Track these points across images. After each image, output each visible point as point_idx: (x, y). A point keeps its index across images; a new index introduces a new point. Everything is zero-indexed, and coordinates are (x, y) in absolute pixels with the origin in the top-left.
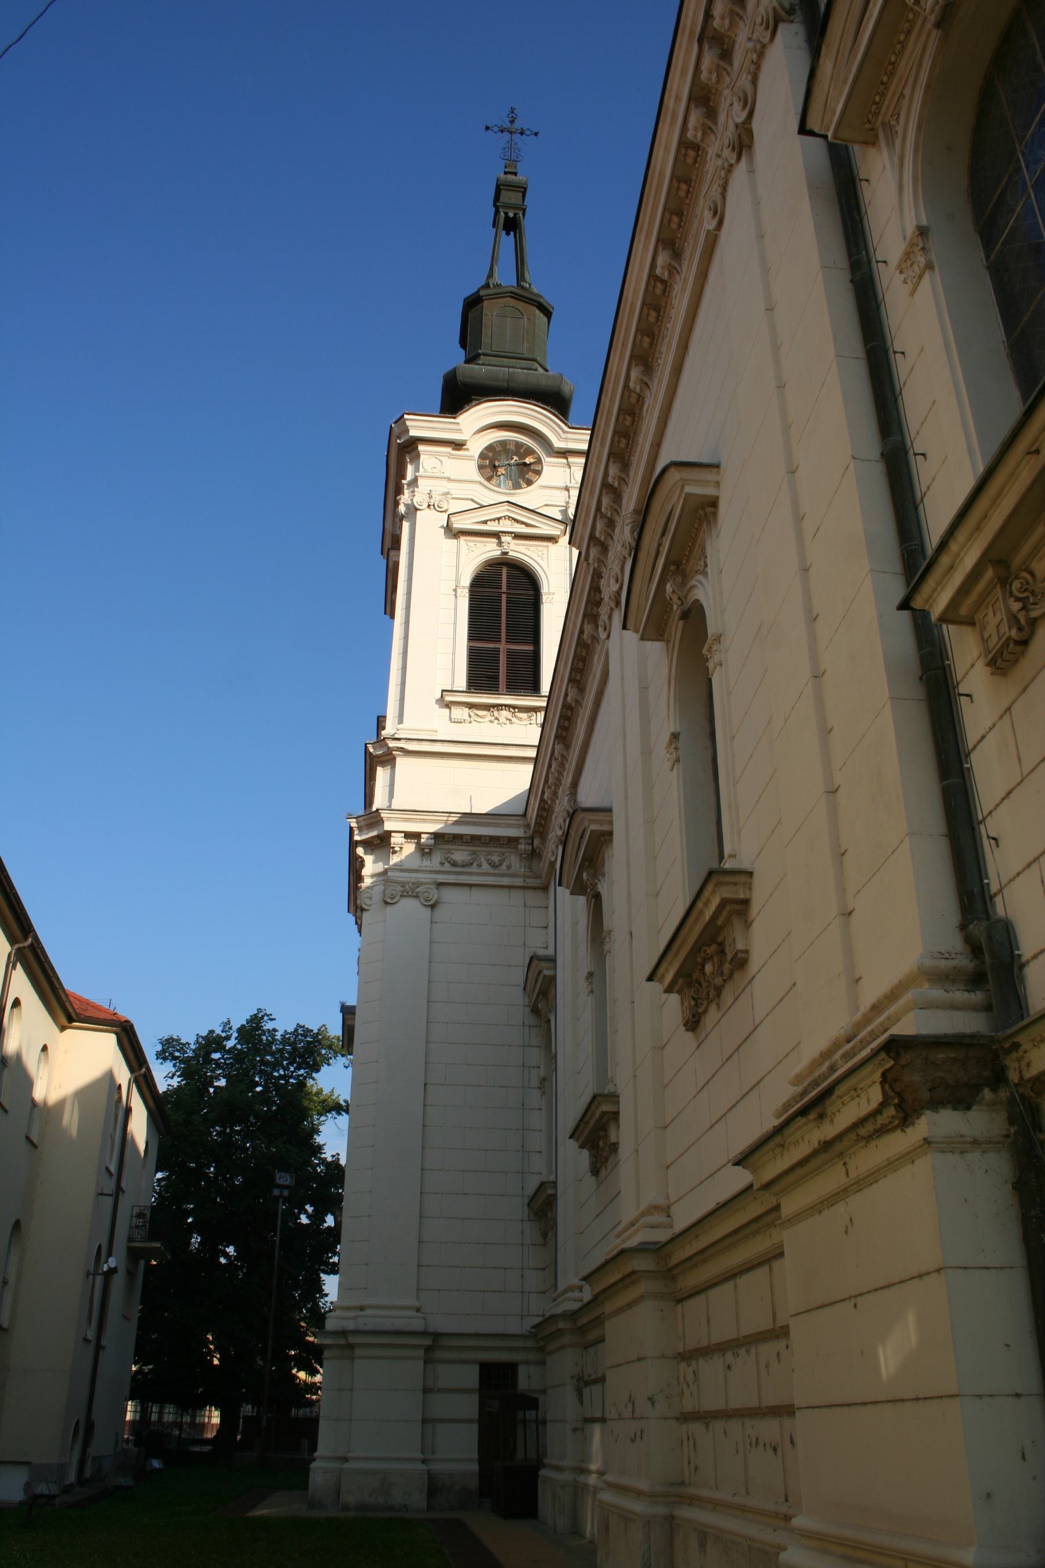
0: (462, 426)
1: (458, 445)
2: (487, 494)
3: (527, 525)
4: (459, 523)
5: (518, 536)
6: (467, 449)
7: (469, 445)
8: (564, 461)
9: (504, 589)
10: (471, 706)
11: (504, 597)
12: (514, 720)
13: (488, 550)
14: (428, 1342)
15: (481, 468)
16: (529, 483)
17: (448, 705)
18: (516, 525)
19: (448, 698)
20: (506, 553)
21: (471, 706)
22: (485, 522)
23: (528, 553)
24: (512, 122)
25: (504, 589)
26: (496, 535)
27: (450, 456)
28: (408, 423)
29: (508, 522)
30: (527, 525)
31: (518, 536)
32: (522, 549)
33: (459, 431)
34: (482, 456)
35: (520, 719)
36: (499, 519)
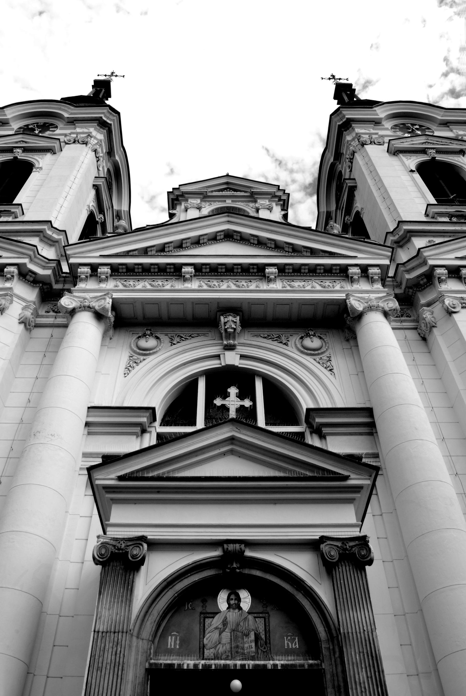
20: (16, 158)
23: (31, 156)
26: (10, 150)
31: (26, 150)
33: (5, 115)
34: (20, 128)
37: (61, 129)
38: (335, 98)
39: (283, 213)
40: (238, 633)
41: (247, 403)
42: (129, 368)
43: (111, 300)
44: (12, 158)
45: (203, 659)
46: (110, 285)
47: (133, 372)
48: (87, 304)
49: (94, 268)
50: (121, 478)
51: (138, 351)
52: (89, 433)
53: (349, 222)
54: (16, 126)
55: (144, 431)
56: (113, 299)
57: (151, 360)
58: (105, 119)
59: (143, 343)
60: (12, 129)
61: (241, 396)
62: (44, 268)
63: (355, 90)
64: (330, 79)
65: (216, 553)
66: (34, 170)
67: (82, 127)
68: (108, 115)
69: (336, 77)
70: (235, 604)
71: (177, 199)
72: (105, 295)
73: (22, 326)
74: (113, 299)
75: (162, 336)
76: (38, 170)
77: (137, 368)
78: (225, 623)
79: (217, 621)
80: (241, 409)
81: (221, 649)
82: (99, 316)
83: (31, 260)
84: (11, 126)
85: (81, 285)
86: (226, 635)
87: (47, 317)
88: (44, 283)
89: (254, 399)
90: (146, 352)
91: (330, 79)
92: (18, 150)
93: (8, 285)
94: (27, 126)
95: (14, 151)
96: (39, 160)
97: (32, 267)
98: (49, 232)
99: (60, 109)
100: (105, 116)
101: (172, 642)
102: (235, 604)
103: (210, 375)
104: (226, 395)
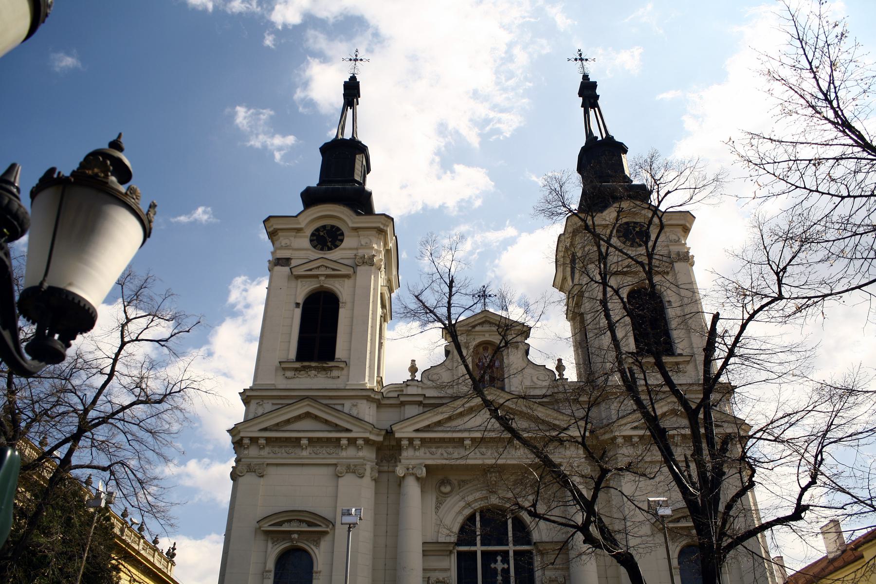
1: (299, 230)
2: (315, 254)
3: (334, 270)
4: (297, 272)
5: (328, 276)
10: (296, 369)
15: (311, 241)
16: (336, 246)
17: (284, 369)
19: (284, 365)
21: (296, 369)
22: (310, 270)
26: (317, 276)
27: (295, 237)
29: (324, 269)
30: (334, 270)
33: (299, 223)
34: (313, 235)
36: (318, 267)
38: (580, 94)
39: (526, 347)
41: (506, 566)
42: (437, 508)
46: (420, 453)
49: (411, 440)
52: (424, 555)
54: (309, 232)
55: (451, 552)
56: (426, 466)
57: (450, 501)
58: (382, 227)
59: (443, 489)
61: (503, 562)
62: (378, 435)
64: (576, 60)
72: (421, 464)
73: (373, 483)
74: (426, 466)
80: (503, 569)
82: (418, 479)
83: (370, 432)
85: (404, 454)
89: (508, 564)
91: (576, 60)
92: (323, 278)
93: (361, 454)
94: (317, 230)
96: (339, 287)
97: (372, 437)
98: (373, 396)
103: (482, 512)
104: (496, 562)
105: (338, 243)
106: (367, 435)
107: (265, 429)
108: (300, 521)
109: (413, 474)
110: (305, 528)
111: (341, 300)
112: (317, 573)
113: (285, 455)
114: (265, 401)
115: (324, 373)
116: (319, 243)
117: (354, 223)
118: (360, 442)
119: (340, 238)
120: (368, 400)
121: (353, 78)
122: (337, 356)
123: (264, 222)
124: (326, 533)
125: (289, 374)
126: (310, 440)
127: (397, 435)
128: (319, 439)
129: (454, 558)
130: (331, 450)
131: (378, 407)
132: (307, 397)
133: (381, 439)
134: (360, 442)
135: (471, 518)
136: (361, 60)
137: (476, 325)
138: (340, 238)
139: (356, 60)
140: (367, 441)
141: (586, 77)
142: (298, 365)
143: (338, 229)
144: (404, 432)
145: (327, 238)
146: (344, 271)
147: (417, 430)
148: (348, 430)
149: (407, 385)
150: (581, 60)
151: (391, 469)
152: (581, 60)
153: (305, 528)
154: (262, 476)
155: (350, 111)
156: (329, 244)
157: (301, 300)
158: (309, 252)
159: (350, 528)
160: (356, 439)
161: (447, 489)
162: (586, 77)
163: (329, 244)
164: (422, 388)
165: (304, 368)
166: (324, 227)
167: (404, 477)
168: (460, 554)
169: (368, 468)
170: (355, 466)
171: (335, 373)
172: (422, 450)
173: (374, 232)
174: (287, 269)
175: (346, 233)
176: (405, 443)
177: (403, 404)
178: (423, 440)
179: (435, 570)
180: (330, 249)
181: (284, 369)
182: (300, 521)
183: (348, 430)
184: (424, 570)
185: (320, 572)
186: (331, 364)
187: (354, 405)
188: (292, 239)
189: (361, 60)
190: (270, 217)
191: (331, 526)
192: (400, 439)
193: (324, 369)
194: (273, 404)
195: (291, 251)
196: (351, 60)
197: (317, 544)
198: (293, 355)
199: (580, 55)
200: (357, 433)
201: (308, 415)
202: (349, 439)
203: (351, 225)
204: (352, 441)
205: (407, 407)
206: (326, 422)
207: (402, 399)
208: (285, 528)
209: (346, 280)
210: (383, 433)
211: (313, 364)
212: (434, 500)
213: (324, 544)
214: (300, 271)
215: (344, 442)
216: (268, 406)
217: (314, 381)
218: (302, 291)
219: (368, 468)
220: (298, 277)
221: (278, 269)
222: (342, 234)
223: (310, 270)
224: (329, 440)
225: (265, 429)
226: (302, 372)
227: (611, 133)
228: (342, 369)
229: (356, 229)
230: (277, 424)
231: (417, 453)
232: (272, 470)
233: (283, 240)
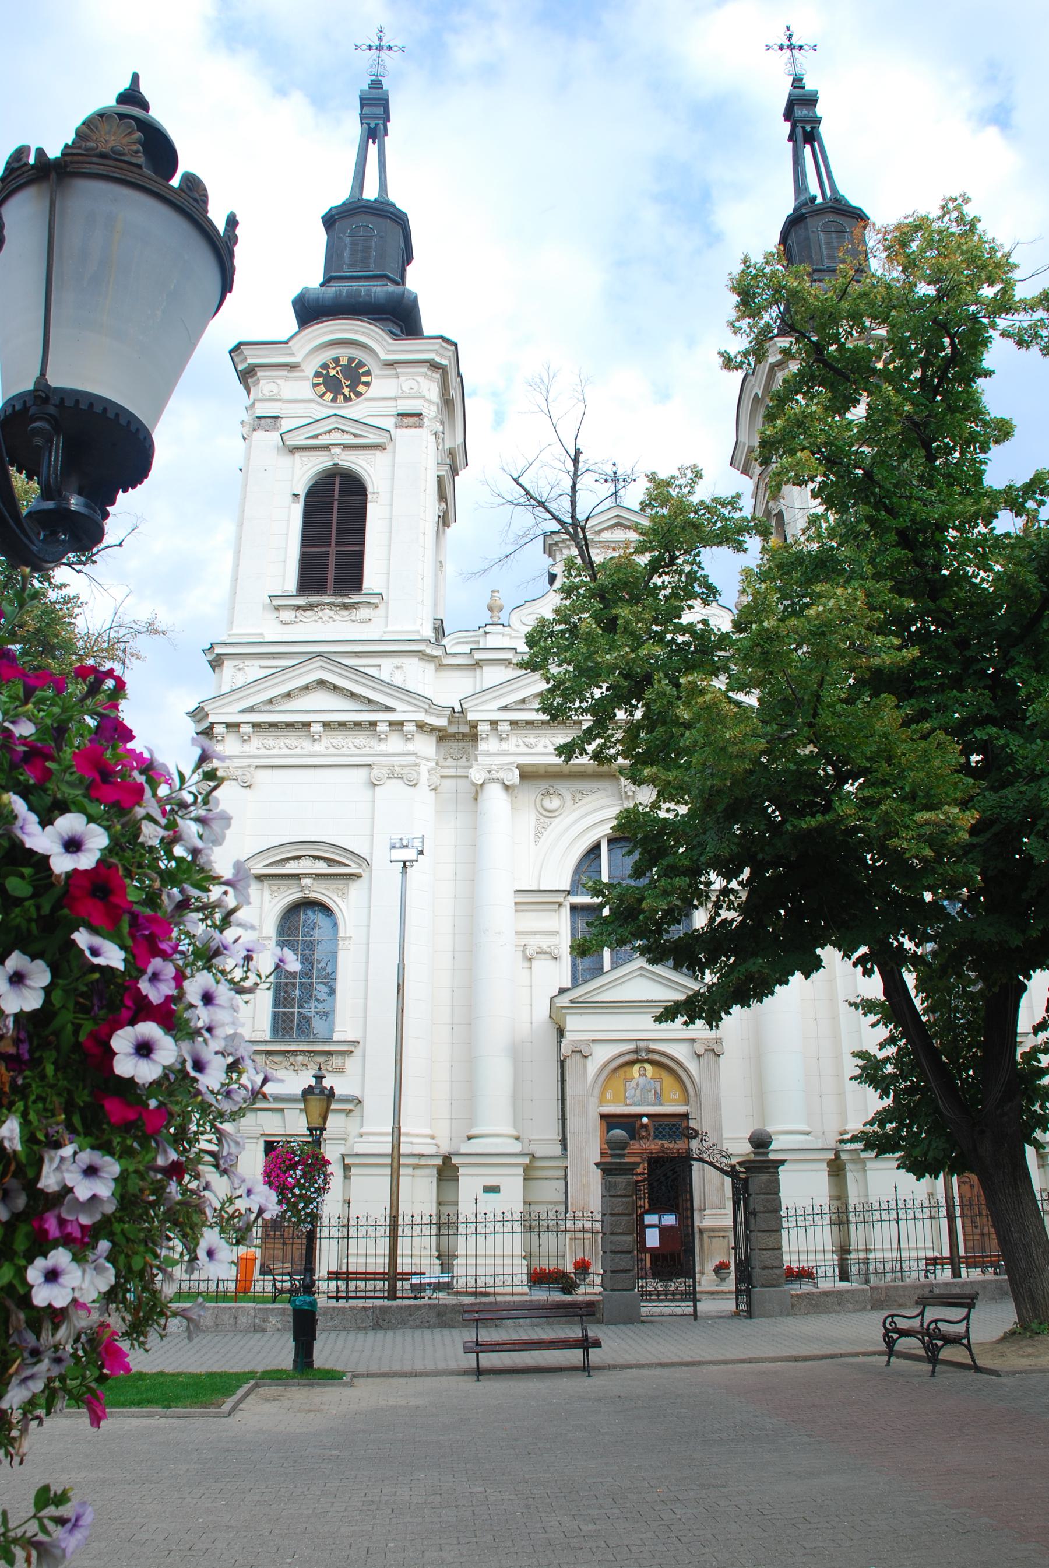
0: (294, 349)
1: (293, 367)
2: (320, 411)
3: (355, 436)
5: (346, 447)
6: (303, 371)
7: (303, 366)
8: (394, 372)
9: (336, 496)
10: (298, 608)
11: (336, 503)
12: (336, 617)
13: (320, 463)
14: (526, 1160)
15: (315, 385)
16: (359, 395)
18: (346, 436)
19: (276, 602)
21: (298, 608)
22: (316, 436)
24: (380, 39)
25: (336, 496)
26: (326, 448)
27: (287, 379)
28: (245, 352)
30: (355, 436)
31: (346, 447)
32: (353, 458)
34: (317, 375)
35: (342, 616)
36: (329, 432)
37: (379, 377)
40: (645, 1090)
42: (538, 835)
43: (517, 772)
44: (331, 463)
45: (627, 1105)
47: (543, 838)
48: (494, 776)
49: (494, 723)
50: (571, 1002)
51: (545, 813)
53: (774, 513)
54: (311, 368)
55: (560, 905)
58: (438, 359)
59: (547, 804)
60: (306, 378)
62: (439, 716)
63: (818, 121)
65: (632, 1046)
66: (369, 497)
67: (406, 374)
68: (442, 351)
69: (794, 41)
70: (643, 1075)
71: (556, 544)
72: (511, 763)
75: (563, 792)
76: (375, 496)
77: (546, 833)
78: (637, 1085)
79: (633, 1083)
81: (636, 1099)
82: (507, 788)
84: (303, 371)
85: (483, 746)
86: (638, 1091)
87: (448, 767)
88: (440, 731)
90: (550, 814)
93: (410, 747)
94: (325, 366)
95: (333, 451)
98: (428, 651)
99: (368, 335)
100: (437, 352)
101: (608, 1096)
102: (643, 1075)
105: (361, 388)
106: (421, 716)
107: (251, 710)
108: (315, 857)
109: (498, 780)
110: (321, 868)
111: (370, 489)
112: (344, 939)
113: (285, 751)
114: (248, 662)
115: (345, 613)
116: (328, 390)
117: (389, 352)
118: (410, 727)
119: (364, 379)
120: (420, 659)
121: (376, 85)
122: (365, 585)
123: (230, 353)
124: (358, 876)
125: (288, 615)
126: (326, 725)
127: (471, 716)
128: (342, 724)
129: (566, 912)
130: (361, 739)
131: (437, 670)
132: (320, 655)
133: (442, 722)
134: (410, 727)
135: (596, 848)
136: (390, 48)
137: (602, 531)
138: (364, 379)
139: (379, 48)
140: (421, 726)
141: (797, 82)
142: (301, 601)
143: (361, 364)
144: (480, 712)
145: (343, 380)
146: (373, 438)
147: (505, 708)
148: (388, 709)
149: (486, 633)
150: (791, 47)
151: (461, 772)
152: (791, 47)
153: (321, 868)
154: (249, 786)
155: (373, 149)
156: (346, 391)
157: (302, 492)
158: (312, 405)
159: (405, 866)
160: (401, 724)
161: (554, 803)
162: (797, 82)
163: (346, 391)
164: (511, 637)
165: (310, 607)
166: (336, 361)
167: (482, 785)
168: (574, 908)
169: (424, 768)
170: (402, 766)
171: (363, 613)
172: (513, 740)
173: (424, 369)
174: (275, 436)
175: (376, 371)
176: (484, 728)
177: (478, 664)
178: (514, 723)
179: (535, 933)
180: (347, 399)
181: (277, 608)
182: (315, 857)
183: (388, 709)
184: (517, 933)
185: (350, 938)
186: (356, 598)
187: (397, 667)
188: (280, 382)
189: (390, 48)
190: (240, 344)
191: (365, 865)
192: (474, 725)
193: (345, 607)
194: (261, 667)
195: (279, 404)
196: (370, 48)
197: (344, 895)
198: (291, 583)
199: (790, 38)
200: (404, 712)
201: (321, 683)
202: (391, 724)
203: (384, 356)
204: (397, 725)
205: (485, 668)
206: (353, 695)
207: (478, 656)
208: (291, 868)
209: (378, 453)
210: (448, 712)
211: (327, 599)
212: (533, 822)
213: (355, 889)
214: (299, 439)
215: (382, 728)
216: (254, 670)
217: (328, 625)
218: (304, 472)
219: (424, 768)
220: (294, 450)
221: (259, 435)
222: (368, 373)
223: (316, 436)
224: (358, 724)
225: (251, 710)
226: (308, 613)
227: (844, 190)
228: (377, 607)
229: (391, 364)
230: (270, 701)
231: (505, 746)
232: (262, 775)
233: (266, 384)
